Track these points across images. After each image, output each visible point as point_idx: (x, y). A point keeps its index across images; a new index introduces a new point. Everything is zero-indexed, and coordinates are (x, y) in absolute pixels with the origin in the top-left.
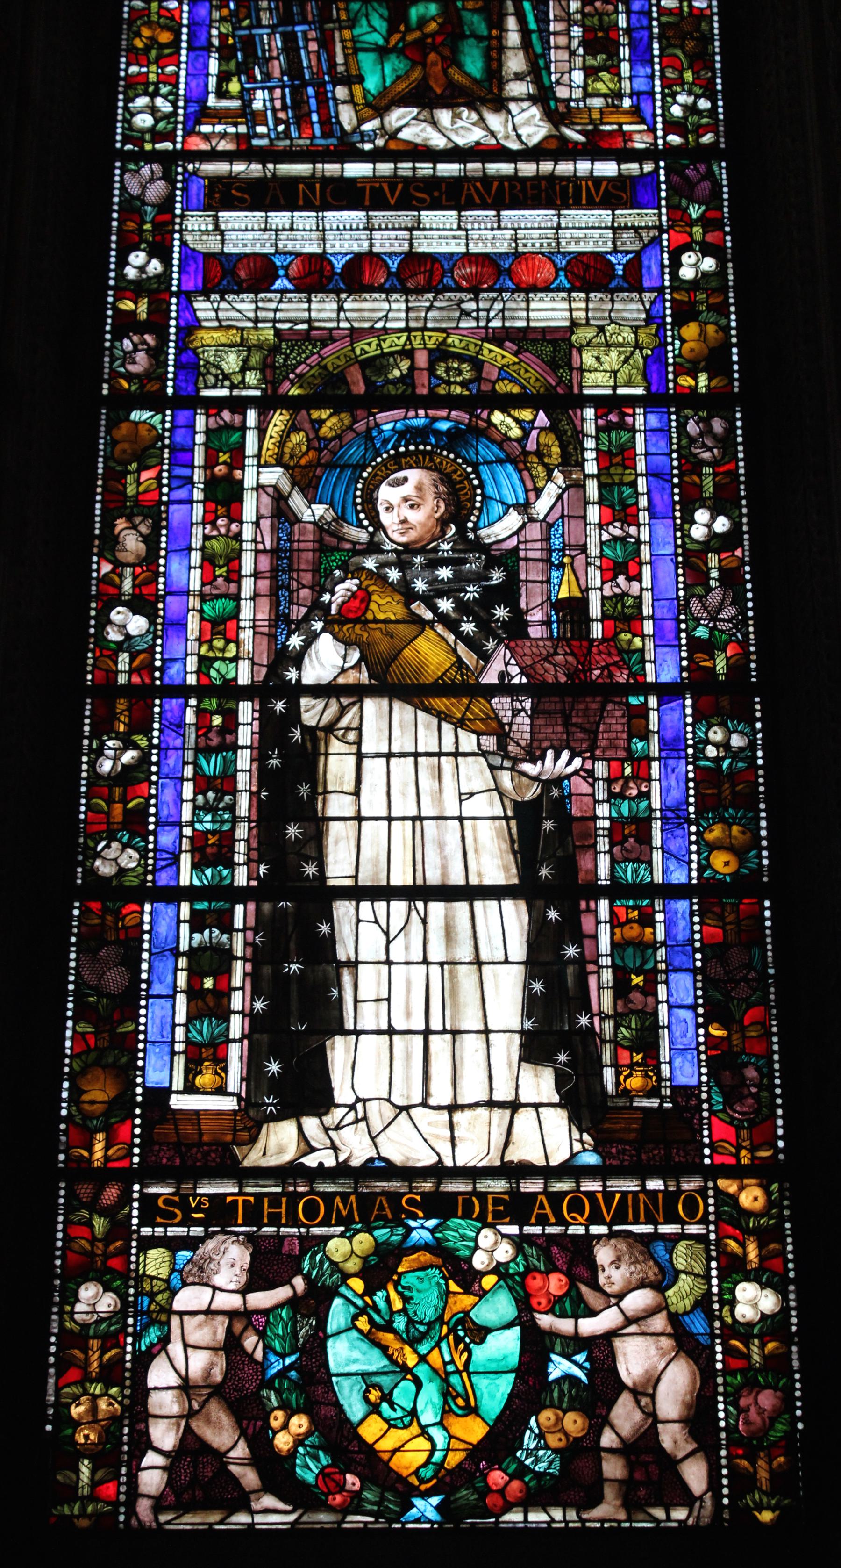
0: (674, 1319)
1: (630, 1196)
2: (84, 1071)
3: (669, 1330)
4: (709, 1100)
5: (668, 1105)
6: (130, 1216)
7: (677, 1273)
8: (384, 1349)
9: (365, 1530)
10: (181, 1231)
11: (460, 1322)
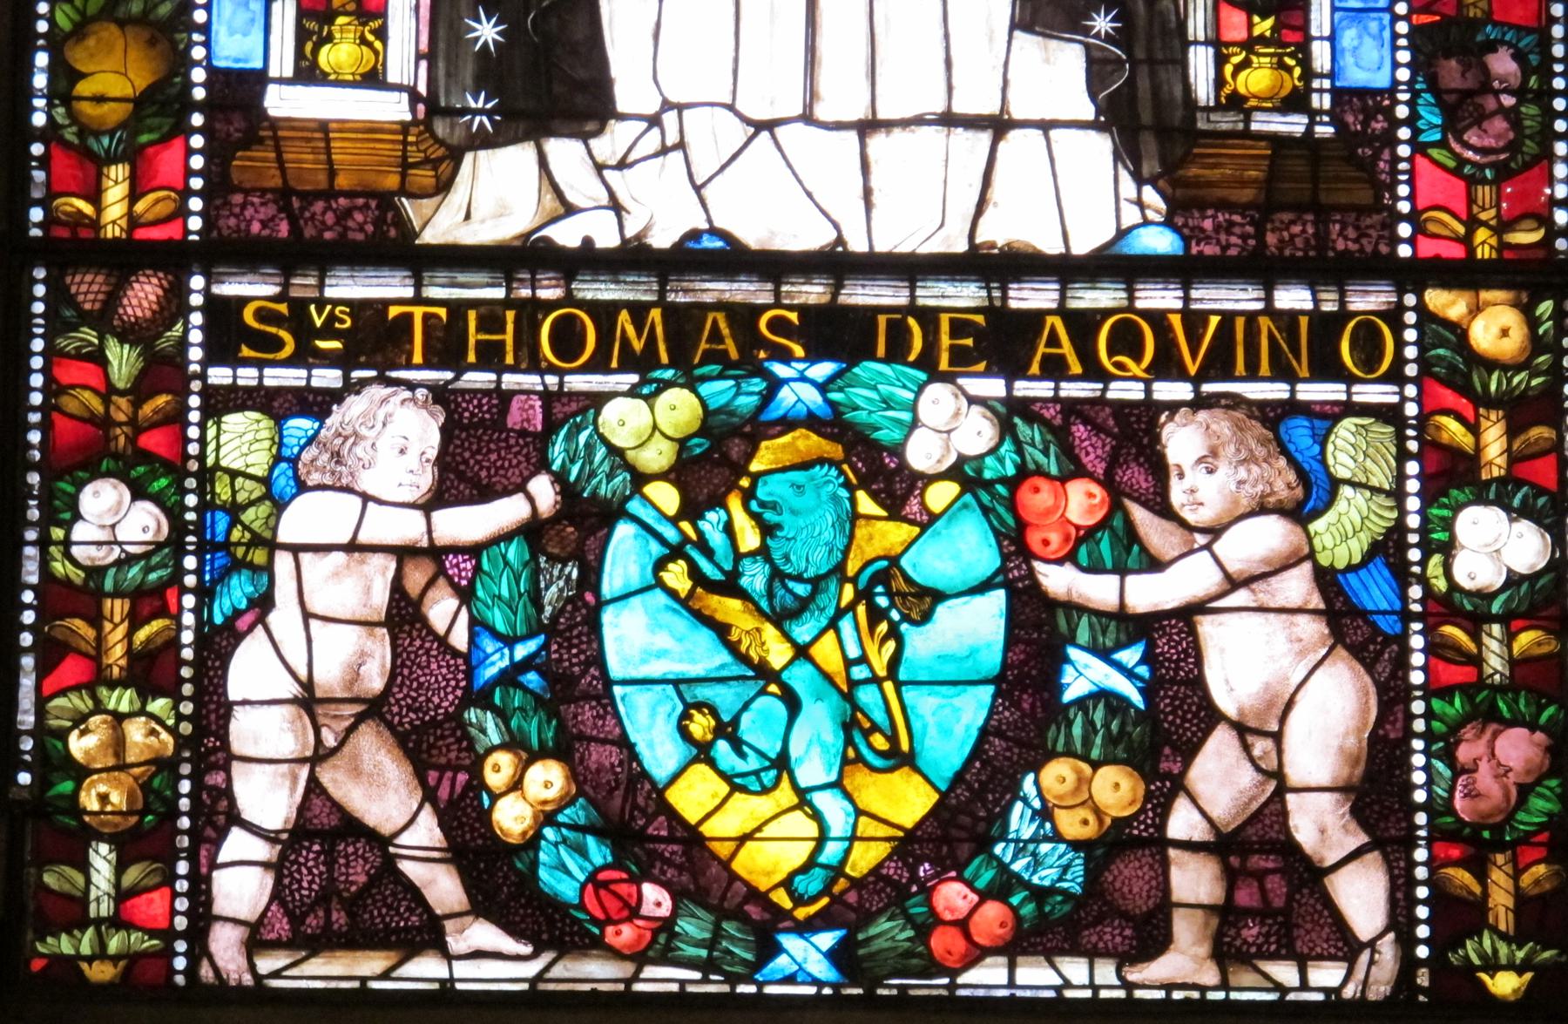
0: (1326, 579)
1: (1240, 323)
2: (80, 30)
3: (1316, 602)
4: (1411, 121)
5: (1324, 131)
6: (183, 343)
7: (1335, 484)
8: (721, 630)
9: (681, 1000)
10: (292, 377)
11: (883, 577)
